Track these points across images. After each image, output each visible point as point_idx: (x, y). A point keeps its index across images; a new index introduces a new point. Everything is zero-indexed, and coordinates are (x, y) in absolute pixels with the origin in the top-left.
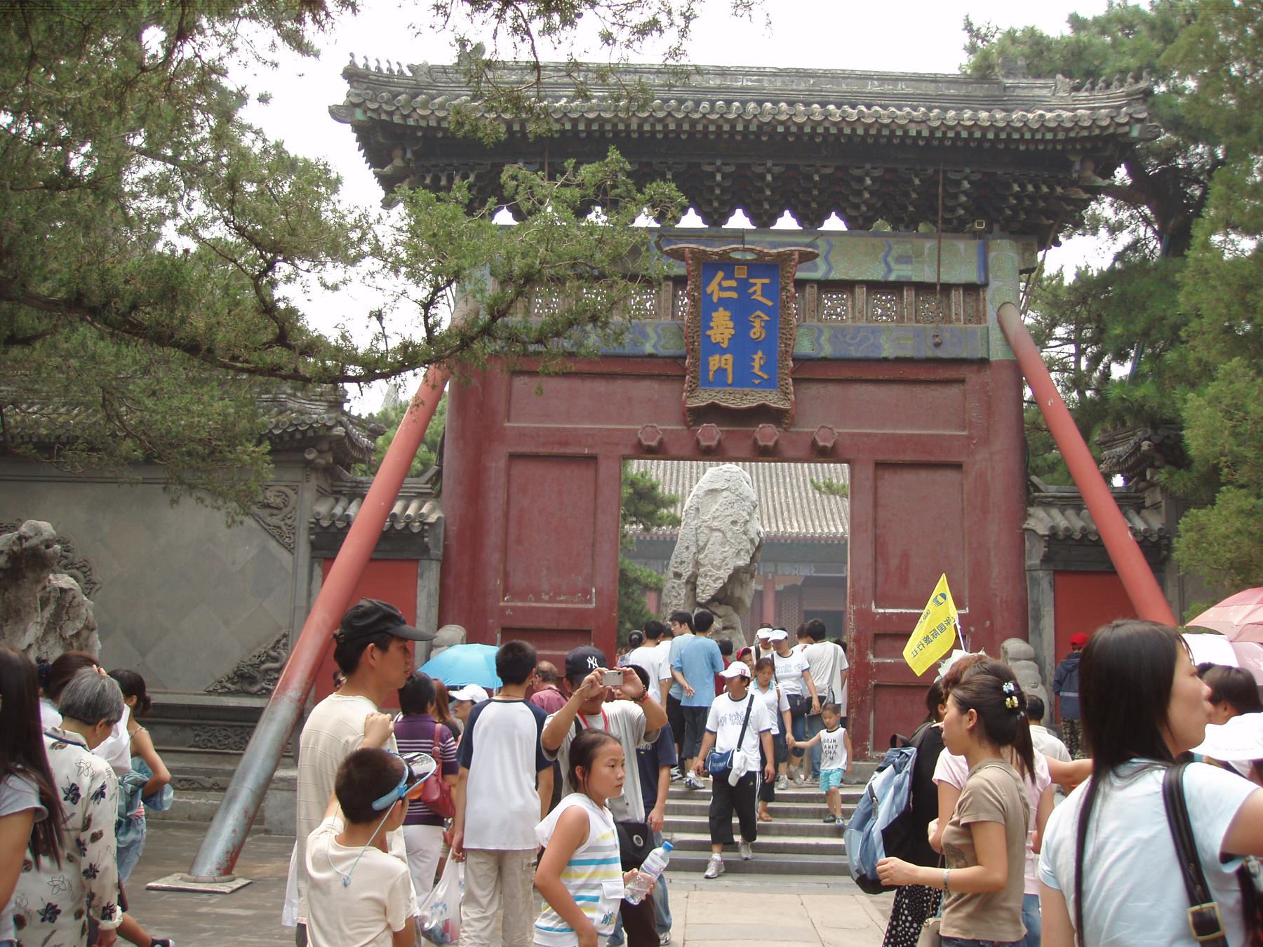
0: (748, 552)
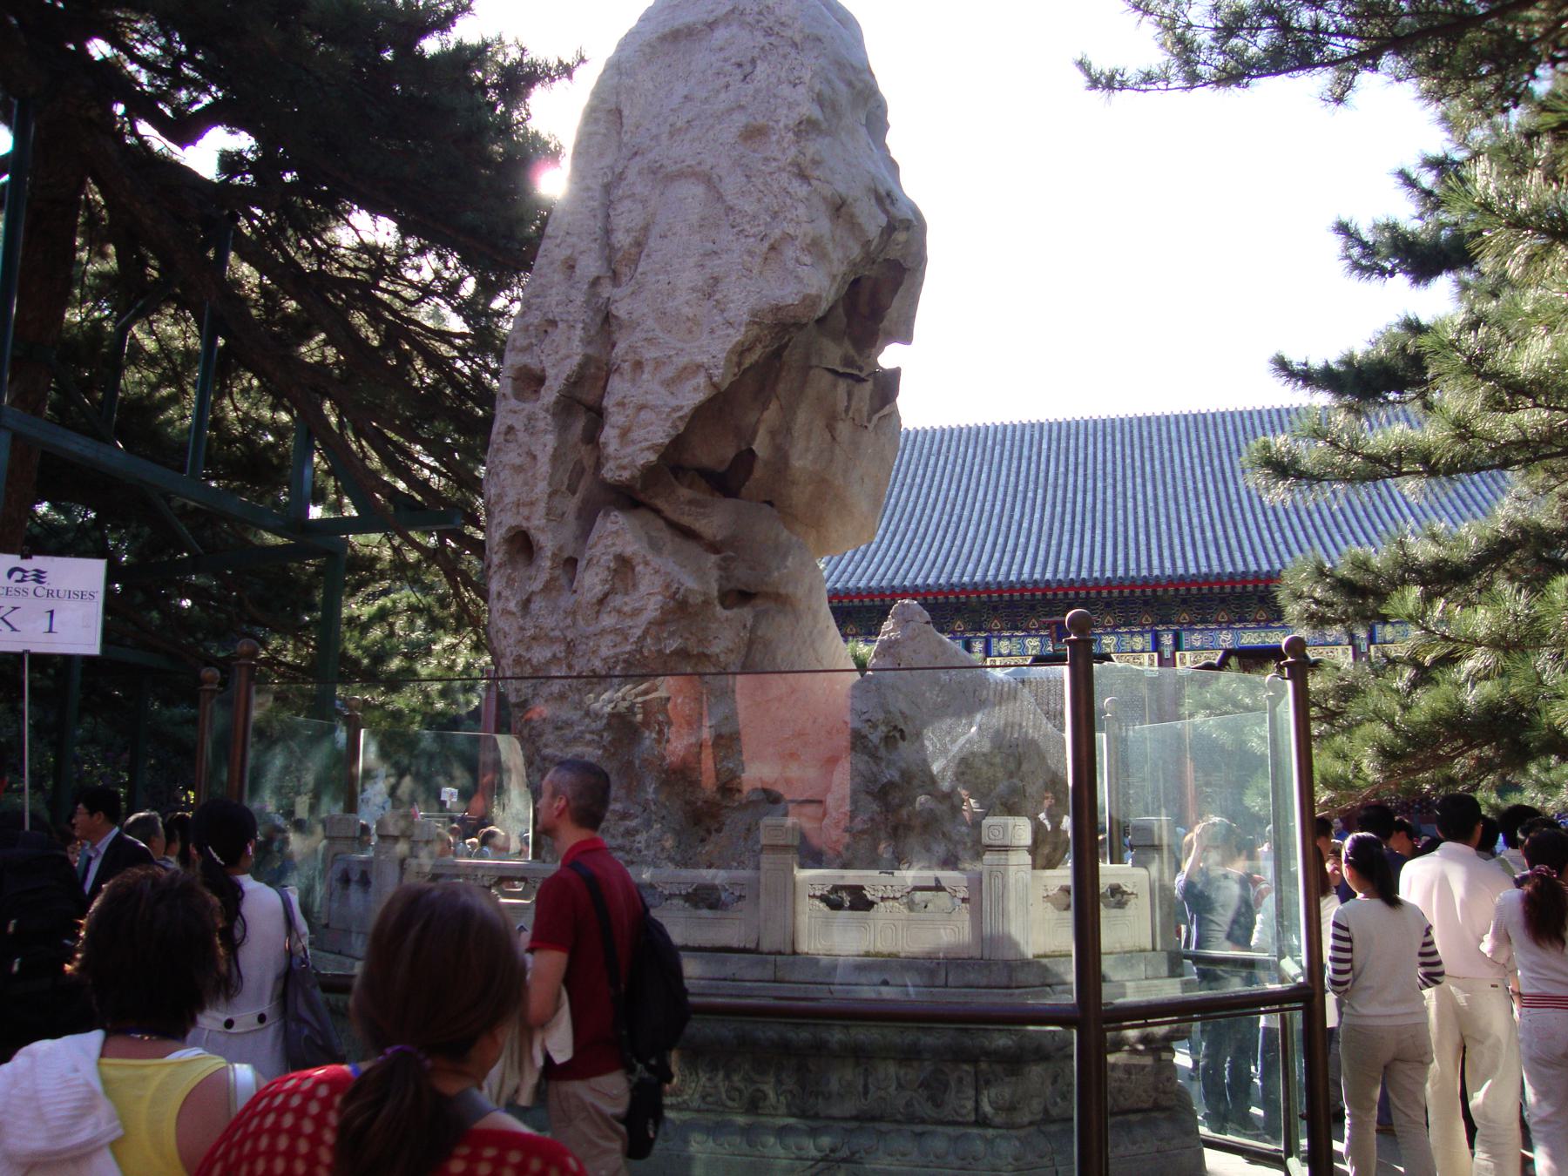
0: (815, 247)
